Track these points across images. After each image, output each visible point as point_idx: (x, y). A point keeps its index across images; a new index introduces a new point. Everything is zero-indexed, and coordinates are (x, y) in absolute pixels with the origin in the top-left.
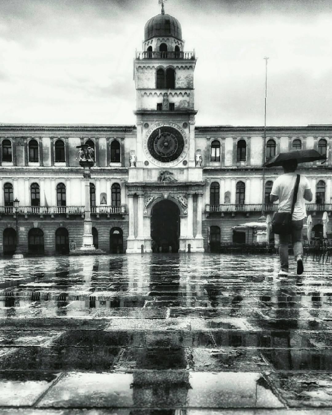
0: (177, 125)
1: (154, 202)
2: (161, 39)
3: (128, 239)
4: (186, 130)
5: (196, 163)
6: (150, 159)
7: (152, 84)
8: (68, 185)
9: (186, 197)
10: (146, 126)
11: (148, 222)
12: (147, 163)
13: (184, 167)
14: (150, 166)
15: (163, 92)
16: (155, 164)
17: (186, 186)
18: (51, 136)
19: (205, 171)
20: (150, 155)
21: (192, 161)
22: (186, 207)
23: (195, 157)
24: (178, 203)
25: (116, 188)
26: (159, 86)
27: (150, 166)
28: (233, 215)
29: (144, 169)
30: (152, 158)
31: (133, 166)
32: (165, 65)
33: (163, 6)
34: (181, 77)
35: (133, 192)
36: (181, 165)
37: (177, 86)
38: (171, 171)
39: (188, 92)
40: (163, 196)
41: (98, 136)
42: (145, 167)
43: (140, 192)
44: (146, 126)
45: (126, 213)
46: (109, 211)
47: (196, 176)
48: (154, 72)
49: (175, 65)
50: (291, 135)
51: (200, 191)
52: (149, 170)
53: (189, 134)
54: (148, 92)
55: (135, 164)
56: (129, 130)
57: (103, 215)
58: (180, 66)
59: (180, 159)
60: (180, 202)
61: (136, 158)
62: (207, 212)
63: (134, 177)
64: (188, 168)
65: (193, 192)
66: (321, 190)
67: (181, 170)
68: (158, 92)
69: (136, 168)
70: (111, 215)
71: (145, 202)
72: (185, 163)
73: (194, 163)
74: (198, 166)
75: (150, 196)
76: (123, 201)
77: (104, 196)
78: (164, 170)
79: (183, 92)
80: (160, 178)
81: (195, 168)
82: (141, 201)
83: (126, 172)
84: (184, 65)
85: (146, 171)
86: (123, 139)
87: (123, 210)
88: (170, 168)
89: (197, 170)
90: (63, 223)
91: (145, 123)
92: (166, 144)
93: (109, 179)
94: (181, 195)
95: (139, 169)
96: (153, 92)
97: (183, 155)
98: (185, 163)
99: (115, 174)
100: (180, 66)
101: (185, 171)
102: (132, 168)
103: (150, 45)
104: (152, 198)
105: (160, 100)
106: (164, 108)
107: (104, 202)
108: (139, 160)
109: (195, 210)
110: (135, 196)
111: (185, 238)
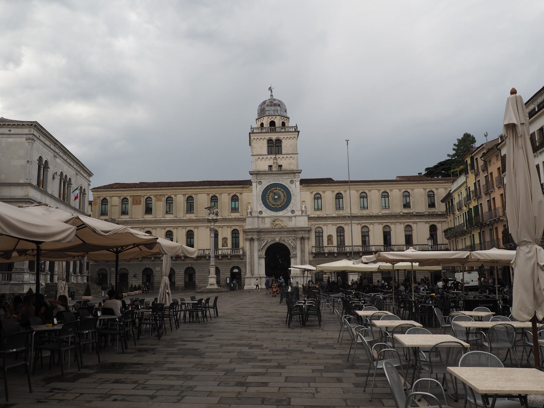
0: (285, 181)
1: (268, 245)
2: (270, 117)
3: (246, 276)
4: (293, 186)
5: (302, 211)
6: (263, 208)
7: (265, 150)
8: (196, 231)
9: (295, 239)
10: (260, 183)
11: (263, 262)
12: (261, 212)
13: (292, 215)
14: (264, 215)
15: (273, 156)
16: (267, 213)
17: (294, 231)
18: (183, 193)
19: (310, 218)
20: (263, 206)
21: (299, 211)
22: (295, 248)
23: (301, 207)
24: (288, 246)
25: (235, 233)
26: (270, 152)
27: (263, 215)
28: (336, 255)
29: (258, 217)
30: (265, 208)
31: (249, 215)
32: (274, 136)
33: (271, 92)
34: (286, 145)
35: (250, 237)
36: (290, 214)
37: (284, 152)
38: (281, 219)
39: (293, 156)
40: (275, 240)
41: (221, 192)
42: (260, 215)
43: (255, 237)
44: (260, 183)
45: (244, 254)
46: (229, 253)
47: (303, 222)
48: (266, 141)
49: (281, 137)
50: (379, 188)
51: (307, 235)
52: (263, 218)
53: (295, 188)
54: (261, 157)
55: (251, 213)
56: (246, 184)
57: (224, 256)
58: (285, 137)
59: (289, 208)
60: (290, 245)
61: (252, 209)
62: (312, 253)
63: (250, 224)
64: (295, 216)
65: (300, 236)
66: (408, 233)
67: (290, 217)
68: (269, 157)
69: (252, 217)
70: (231, 256)
71: (260, 245)
72: (293, 212)
73: (301, 212)
74: (304, 214)
75: (264, 240)
76: (241, 245)
77: (225, 239)
78: (275, 218)
79: (289, 156)
80: (272, 223)
81: (302, 216)
82: (256, 243)
83: (244, 220)
84: (289, 137)
85: (260, 219)
86: (241, 194)
87: (241, 253)
88: (280, 216)
89: (303, 217)
90: (192, 264)
91: (259, 181)
92: (276, 197)
93: (231, 227)
94: (290, 238)
95: (254, 217)
96: (265, 157)
97: (291, 205)
98: (293, 212)
99: (235, 222)
100: (285, 137)
101: (293, 218)
102: (249, 217)
103: (262, 122)
104: (266, 241)
105: (271, 163)
106: (274, 169)
107: (225, 245)
108: (255, 209)
109: (303, 251)
110: (252, 240)
111: (295, 275)
